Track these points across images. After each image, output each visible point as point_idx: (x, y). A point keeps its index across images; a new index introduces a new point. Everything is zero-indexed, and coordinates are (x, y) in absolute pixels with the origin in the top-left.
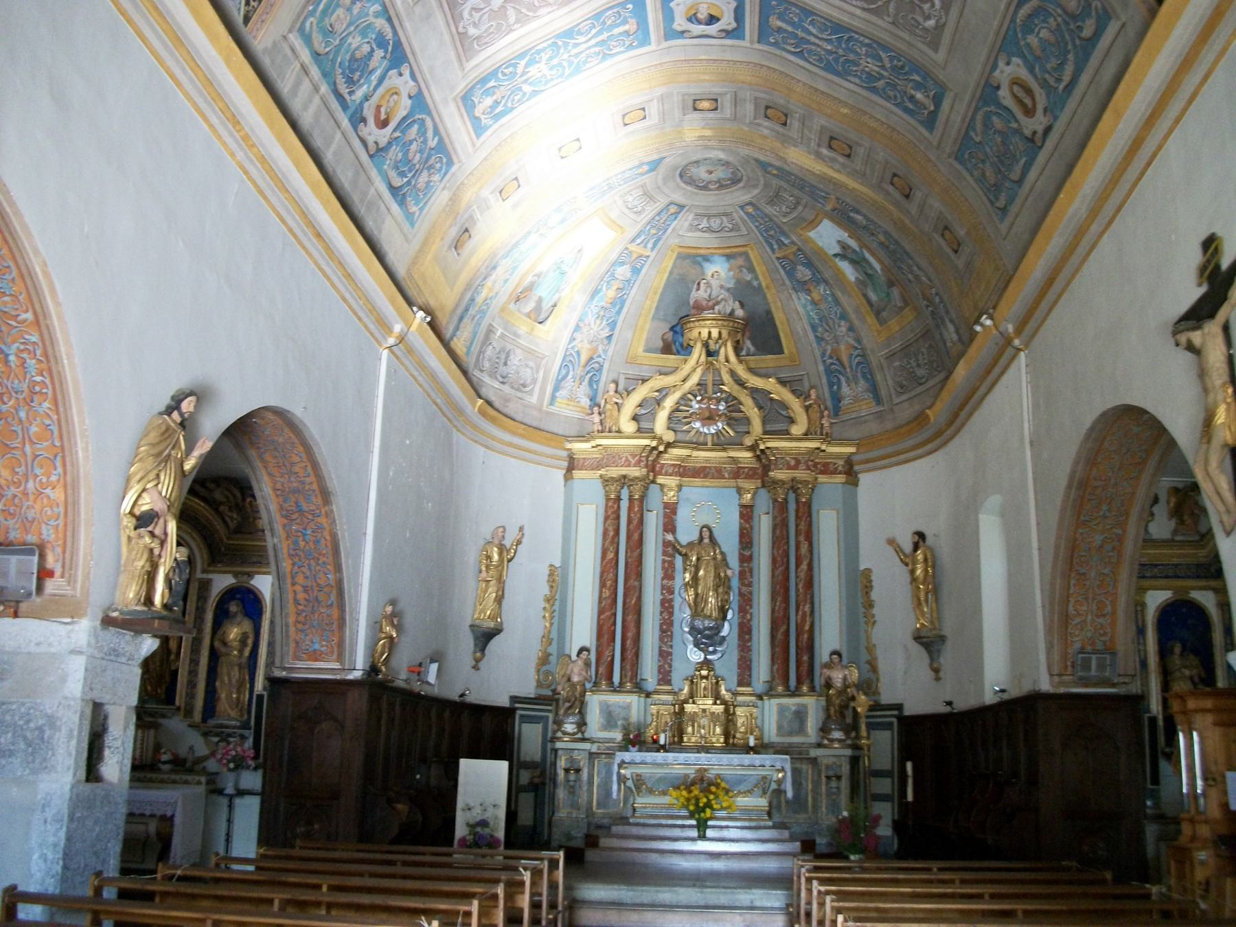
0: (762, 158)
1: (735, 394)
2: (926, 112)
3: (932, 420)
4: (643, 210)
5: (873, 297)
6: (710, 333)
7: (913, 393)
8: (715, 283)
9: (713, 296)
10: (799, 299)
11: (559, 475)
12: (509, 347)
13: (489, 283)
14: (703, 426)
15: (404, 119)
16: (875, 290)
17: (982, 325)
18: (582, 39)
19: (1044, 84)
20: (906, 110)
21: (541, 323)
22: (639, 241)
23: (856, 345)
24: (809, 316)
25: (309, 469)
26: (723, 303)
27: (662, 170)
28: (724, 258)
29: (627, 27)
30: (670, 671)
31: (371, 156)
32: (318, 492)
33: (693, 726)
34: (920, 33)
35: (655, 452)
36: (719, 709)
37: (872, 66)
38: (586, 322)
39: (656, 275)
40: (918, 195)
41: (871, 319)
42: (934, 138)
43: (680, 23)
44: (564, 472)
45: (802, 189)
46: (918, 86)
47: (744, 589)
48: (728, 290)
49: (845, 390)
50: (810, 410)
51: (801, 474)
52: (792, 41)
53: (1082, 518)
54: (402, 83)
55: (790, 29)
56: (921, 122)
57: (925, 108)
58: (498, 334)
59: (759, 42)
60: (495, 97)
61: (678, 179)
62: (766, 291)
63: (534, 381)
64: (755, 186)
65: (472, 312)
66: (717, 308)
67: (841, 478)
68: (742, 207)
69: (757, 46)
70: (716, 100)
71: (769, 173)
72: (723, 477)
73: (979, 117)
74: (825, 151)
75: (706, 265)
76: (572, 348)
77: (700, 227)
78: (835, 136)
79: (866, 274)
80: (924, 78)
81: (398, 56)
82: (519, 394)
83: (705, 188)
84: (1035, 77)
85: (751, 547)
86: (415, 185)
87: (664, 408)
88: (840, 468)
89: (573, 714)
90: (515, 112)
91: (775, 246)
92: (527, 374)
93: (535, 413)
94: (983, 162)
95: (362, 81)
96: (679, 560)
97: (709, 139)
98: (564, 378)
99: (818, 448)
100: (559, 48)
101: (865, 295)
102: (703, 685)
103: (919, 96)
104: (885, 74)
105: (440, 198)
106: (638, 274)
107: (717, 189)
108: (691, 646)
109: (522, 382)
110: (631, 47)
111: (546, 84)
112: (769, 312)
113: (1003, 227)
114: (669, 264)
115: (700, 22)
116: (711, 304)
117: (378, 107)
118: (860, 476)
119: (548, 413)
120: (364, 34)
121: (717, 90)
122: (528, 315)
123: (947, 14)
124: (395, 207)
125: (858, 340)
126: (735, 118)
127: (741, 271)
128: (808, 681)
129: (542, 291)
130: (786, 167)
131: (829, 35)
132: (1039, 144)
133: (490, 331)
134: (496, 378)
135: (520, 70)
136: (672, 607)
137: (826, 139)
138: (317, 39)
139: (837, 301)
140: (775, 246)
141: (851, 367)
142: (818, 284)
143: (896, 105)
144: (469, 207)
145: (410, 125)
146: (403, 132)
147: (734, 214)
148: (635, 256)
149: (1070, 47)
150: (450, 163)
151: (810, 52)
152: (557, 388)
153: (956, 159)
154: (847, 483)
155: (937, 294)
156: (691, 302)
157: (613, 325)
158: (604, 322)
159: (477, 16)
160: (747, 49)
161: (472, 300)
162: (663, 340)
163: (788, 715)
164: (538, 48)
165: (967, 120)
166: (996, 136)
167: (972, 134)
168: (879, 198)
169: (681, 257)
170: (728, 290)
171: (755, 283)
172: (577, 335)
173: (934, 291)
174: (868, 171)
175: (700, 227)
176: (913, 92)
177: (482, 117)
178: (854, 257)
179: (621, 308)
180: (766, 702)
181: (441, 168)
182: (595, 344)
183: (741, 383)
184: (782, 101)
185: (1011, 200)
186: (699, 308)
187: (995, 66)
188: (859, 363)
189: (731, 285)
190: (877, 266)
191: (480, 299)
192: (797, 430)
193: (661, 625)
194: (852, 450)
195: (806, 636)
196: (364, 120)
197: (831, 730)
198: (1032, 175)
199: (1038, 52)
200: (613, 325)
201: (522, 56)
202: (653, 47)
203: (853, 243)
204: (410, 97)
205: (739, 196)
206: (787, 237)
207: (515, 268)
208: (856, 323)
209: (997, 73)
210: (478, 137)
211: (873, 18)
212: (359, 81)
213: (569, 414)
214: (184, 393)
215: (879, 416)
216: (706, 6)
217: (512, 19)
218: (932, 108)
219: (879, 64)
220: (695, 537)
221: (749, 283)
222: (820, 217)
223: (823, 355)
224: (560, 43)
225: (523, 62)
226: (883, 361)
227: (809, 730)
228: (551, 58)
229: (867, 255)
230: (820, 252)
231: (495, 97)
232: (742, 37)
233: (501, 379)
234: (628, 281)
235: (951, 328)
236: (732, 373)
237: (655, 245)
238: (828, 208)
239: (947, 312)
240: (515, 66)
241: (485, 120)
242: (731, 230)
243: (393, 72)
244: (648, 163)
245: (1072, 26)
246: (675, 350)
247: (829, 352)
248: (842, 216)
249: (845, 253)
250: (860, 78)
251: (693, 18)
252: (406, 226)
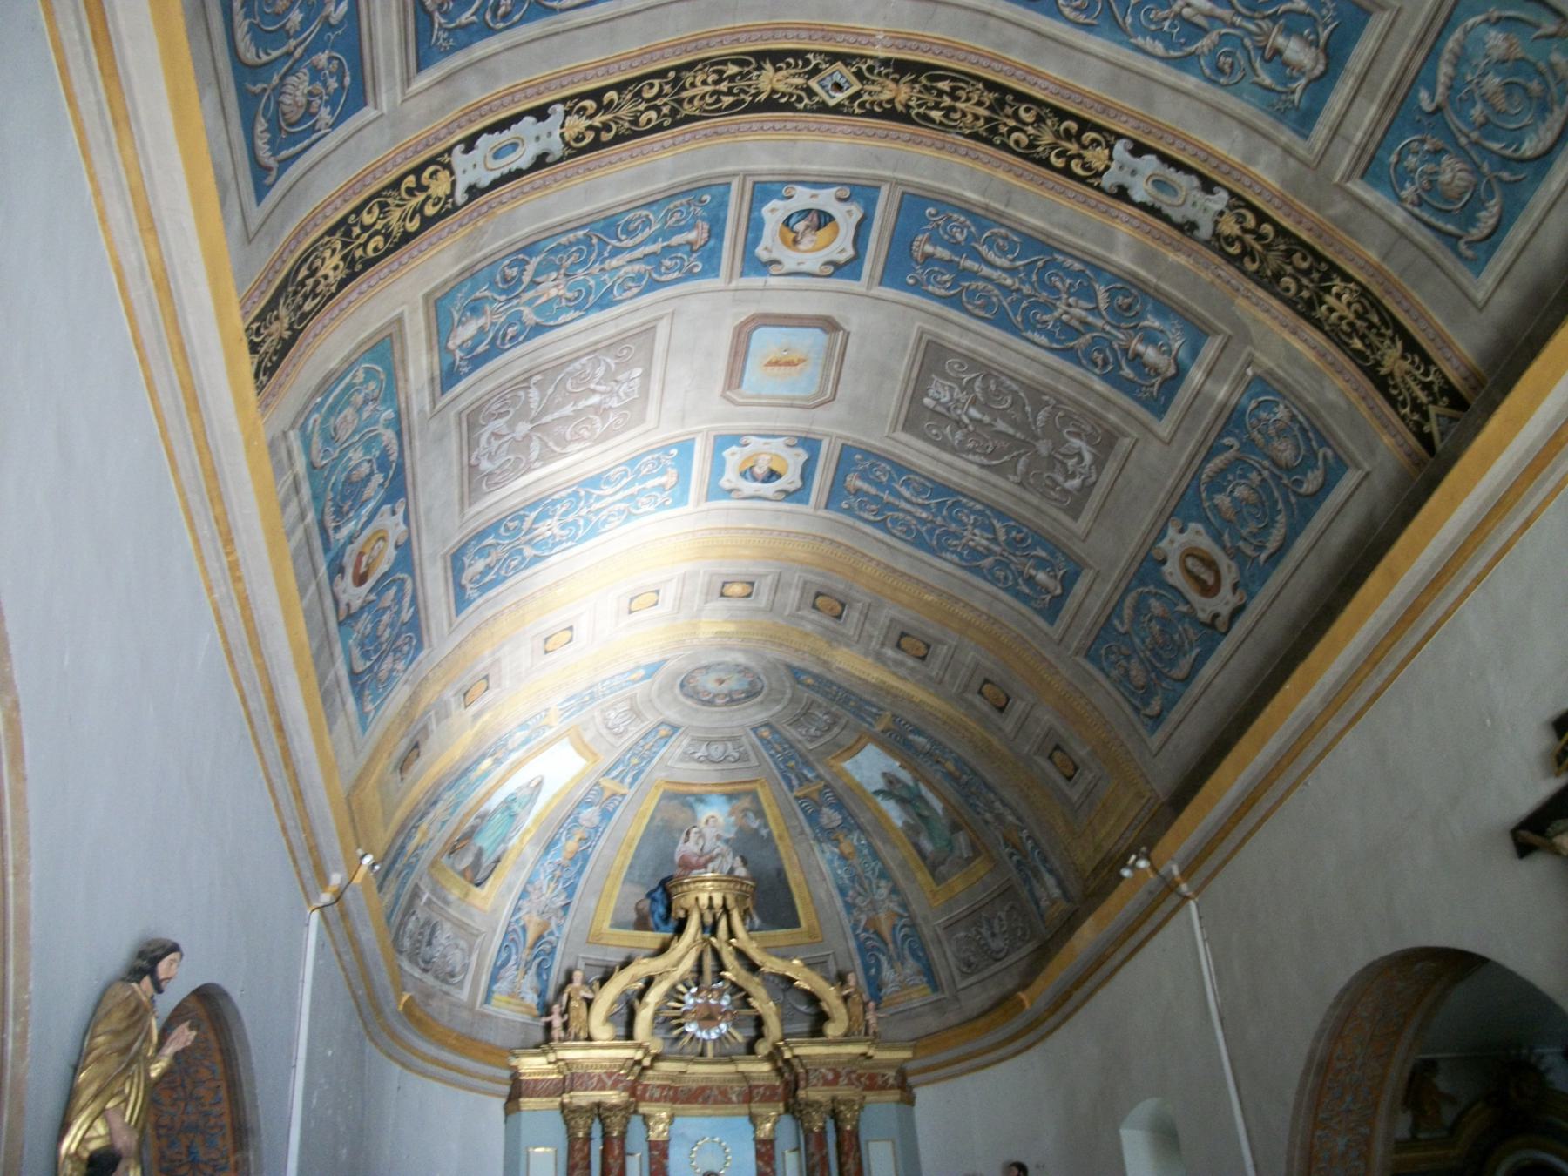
0: (796, 663)
1: (741, 983)
2: (1048, 597)
3: (1027, 1005)
4: (626, 731)
5: (928, 846)
6: (711, 899)
7: (986, 973)
8: (710, 832)
9: (706, 850)
10: (823, 852)
11: (498, 1104)
12: (436, 918)
13: (424, 825)
14: (701, 1028)
15: (385, 576)
16: (931, 838)
17: (1133, 867)
18: (609, 490)
19: (1235, 554)
20: (1018, 595)
21: (478, 885)
22: (614, 773)
23: (901, 911)
24: (836, 876)
25: (223, 1093)
26: (720, 859)
27: (659, 677)
28: (723, 799)
29: (663, 480)
31: (340, 624)
32: (228, 1130)
34: (1057, 496)
35: (637, 1069)
37: (980, 539)
38: (537, 884)
39: (631, 825)
40: (1019, 707)
41: (923, 877)
42: (1056, 631)
43: (730, 478)
44: (503, 1101)
45: (844, 703)
46: (1041, 564)
48: (727, 841)
49: (888, 973)
50: (850, 1001)
51: (843, 1092)
52: (874, 507)
53: (1321, 1115)
54: (392, 525)
55: (873, 491)
56: (1039, 611)
57: (1048, 592)
58: (425, 898)
59: (826, 507)
60: (489, 560)
61: (677, 690)
62: (778, 842)
63: (465, 967)
64: (778, 701)
65: (398, 866)
66: (711, 866)
67: (894, 1095)
68: (755, 730)
69: (823, 513)
70: (752, 584)
71: (799, 682)
72: (729, 1101)
73: (1130, 600)
74: (889, 652)
75: (700, 807)
76: (517, 921)
77: (697, 755)
78: (906, 631)
79: (920, 816)
80: (1052, 554)
81: (397, 488)
82: (445, 988)
83: (710, 703)
84: (1224, 547)
86: (377, 674)
87: (647, 1005)
88: (891, 1081)
90: (508, 583)
91: (795, 782)
92: (456, 958)
93: (465, 1015)
94: (1128, 658)
95: (351, 514)
97: (728, 635)
98: (504, 964)
99: (864, 1055)
100: (579, 499)
101: (916, 846)
103: (1041, 576)
104: (997, 549)
105: (400, 695)
106: (610, 819)
107: (726, 704)
109: (449, 969)
110: (662, 507)
111: (552, 548)
112: (780, 874)
113: (1155, 740)
114: (650, 805)
115: (755, 479)
116: (702, 860)
117: (361, 554)
119: (484, 1016)
120: (367, 448)
121: (761, 569)
122: (463, 873)
123: (1099, 473)
124: (351, 701)
125: (905, 905)
126: (771, 609)
127: (745, 816)
129: (484, 841)
130: (829, 676)
131: (927, 499)
132: (1223, 630)
133: (416, 893)
134: (417, 964)
135: (526, 526)
137: (894, 636)
138: (317, 443)
139: (875, 854)
140: (795, 782)
141: (895, 942)
142: (850, 831)
143: (1006, 590)
144: (426, 712)
145: (387, 587)
146: (379, 595)
147: (744, 740)
148: (607, 794)
149: (1280, 505)
150: (419, 647)
151: (895, 521)
152: (494, 979)
153: (1086, 656)
154: (901, 1101)
155: (1029, 838)
156: (677, 858)
157: (570, 890)
158: (560, 886)
159: (495, 444)
160: (810, 516)
161: (403, 847)
162: (638, 910)
164: (556, 497)
165: (1112, 603)
166: (1152, 624)
167: (1116, 622)
168: (956, 712)
169: (668, 796)
170: (727, 841)
171: (764, 832)
172: (524, 904)
173: (1025, 833)
174: (947, 678)
175: (697, 755)
176: (1033, 572)
177: (469, 586)
178: (904, 793)
179: (583, 867)
181: (408, 652)
182: (545, 916)
183: (753, 968)
184: (841, 587)
185: (1169, 705)
186: (687, 865)
187: (1162, 534)
188: (905, 937)
189: (728, 836)
190: (937, 805)
191: (410, 847)
192: (832, 1030)
194: (906, 1054)
196: (342, 570)
198: (1208, 670)
199: (1230, 515)
200: (570, 890)
201: (533, 506)
202: (689, 508)
203: (905, 776)
204: (397, 547)
205: (755, 714)
206: (812, 769)
207: (457, 805)
208: (902, 882)
209: (1164, 544)
210: (458, 614)
211: (994, 478)
212: (348, 512)
213: (510, 1016)
214: (163, 947)
215: (938, 1007)
216: (768, 457)
217: (534, 454)
218: (1059, 591)
219: (991, 536)
221: (756, 831)
222: (863, 741)
223: (855, 927)
224: (582, 493)
225: (533, 515)
226: (940, 931)
228: (566, 513)
229: (924, 790)
230: (855, 790)
231: (489, 560)
232: (805, 501)
233: (423, 965)
234: (596, 828)
235: (1050, 881)
236: (741, 954)
237: (635, 778)
238: (878, 728)
239: (1045, 860)
240: (522, 519)
241: (471, 592)
242: (736, 761)
243: (387, 508)
244: (646, 667)
245: (1285, 481)
246: (652, 925)
247: (863, 923)
248: (897, 741)
249: (892, 788)
250: (960, 555)
251: (748, 473)
252: (358, 729)
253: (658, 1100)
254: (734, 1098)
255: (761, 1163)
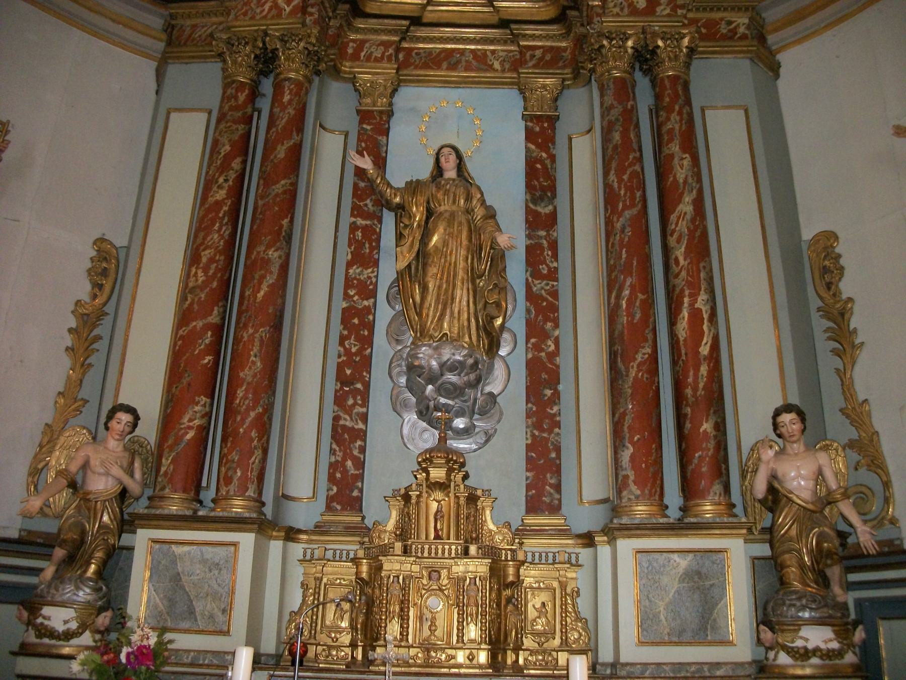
30: (361, 477)
33: (404, 618)
36: (477, 567)
47: (538, 286)
85: (554, 196)
88: (742, 30)
89: (81, 580)
96: (389, 219)
102: (434, 506)
108: (411, 417)
118: (779, 57)
128: (717, 488)
136: (371, 327)
163: (671, 584)
180: (604, 551)
193: (340, 368)
195: (704, 370)
197: (798, 624)
220: (424, 172)
227: (732, 627)
253: (377, 60)
254: (497, 65)
255: (533, 147)
